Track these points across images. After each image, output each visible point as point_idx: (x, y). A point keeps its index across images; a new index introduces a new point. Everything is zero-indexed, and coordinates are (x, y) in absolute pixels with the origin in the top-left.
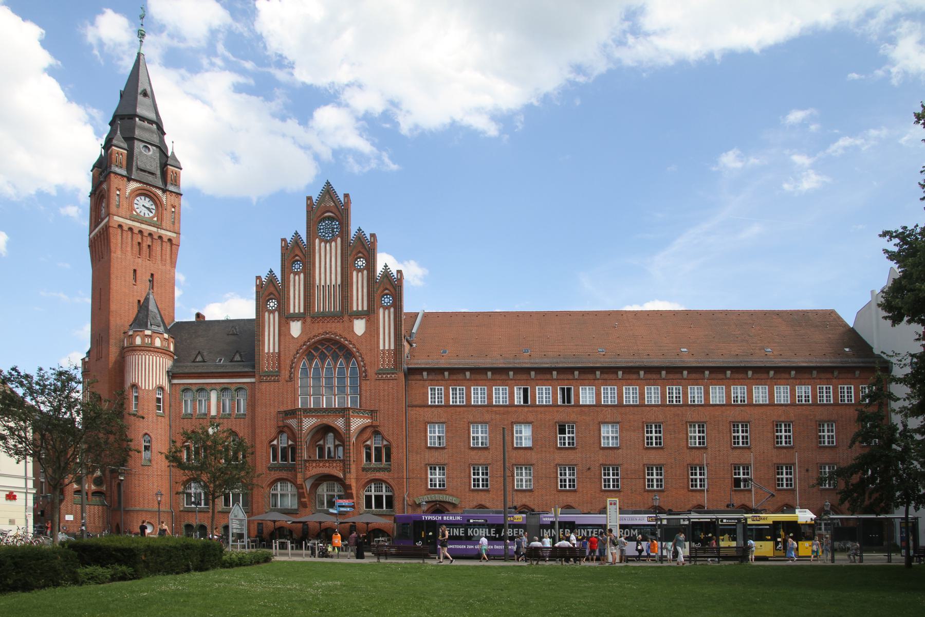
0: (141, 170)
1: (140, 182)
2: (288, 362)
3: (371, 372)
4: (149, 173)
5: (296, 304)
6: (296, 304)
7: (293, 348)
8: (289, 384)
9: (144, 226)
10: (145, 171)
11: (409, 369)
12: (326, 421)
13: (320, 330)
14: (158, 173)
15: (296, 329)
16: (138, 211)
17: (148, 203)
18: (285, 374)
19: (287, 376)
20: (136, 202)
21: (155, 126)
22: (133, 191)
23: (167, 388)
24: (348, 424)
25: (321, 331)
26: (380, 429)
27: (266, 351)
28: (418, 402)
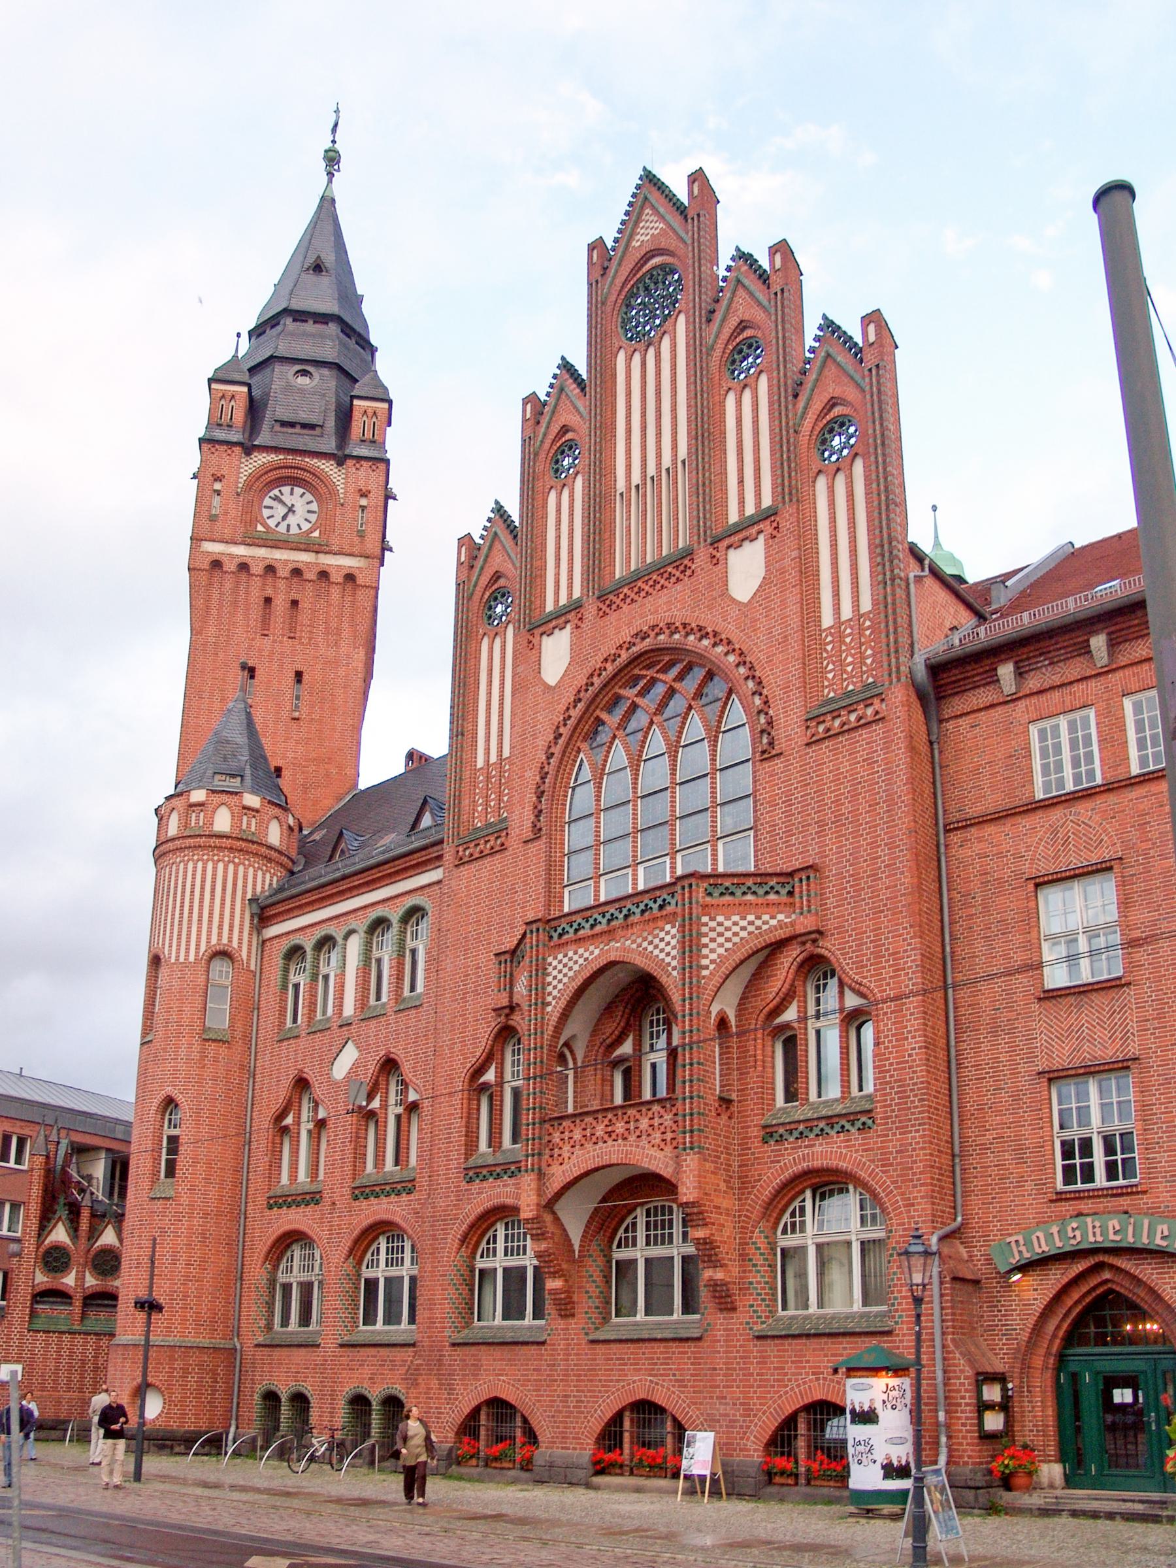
0: (284, 424)
1: (276, 449)
2: (532, 776)
3: (790, 727)
4: (304, 426)
5: (563, 579)
6: (563, 579)
7: (545, 721)
8: (533, 848)
9: (279, 555)
10: (292, 425)
11: (936, 669)
12: (614, 949)
13: (620, 630)
14: (331, 424)
15: (556, 655)
16: (272, 523)
17: (297, 497)
18: (521, 821)
19: (528, 824)
20: (267, 501)
21: (333, 328)
22: (255, 478)
23: (246, 950)
24: (690, 946)
25: (626, 635)
26: (828, 947)
27: (480, 763)
28: (991, 802)
